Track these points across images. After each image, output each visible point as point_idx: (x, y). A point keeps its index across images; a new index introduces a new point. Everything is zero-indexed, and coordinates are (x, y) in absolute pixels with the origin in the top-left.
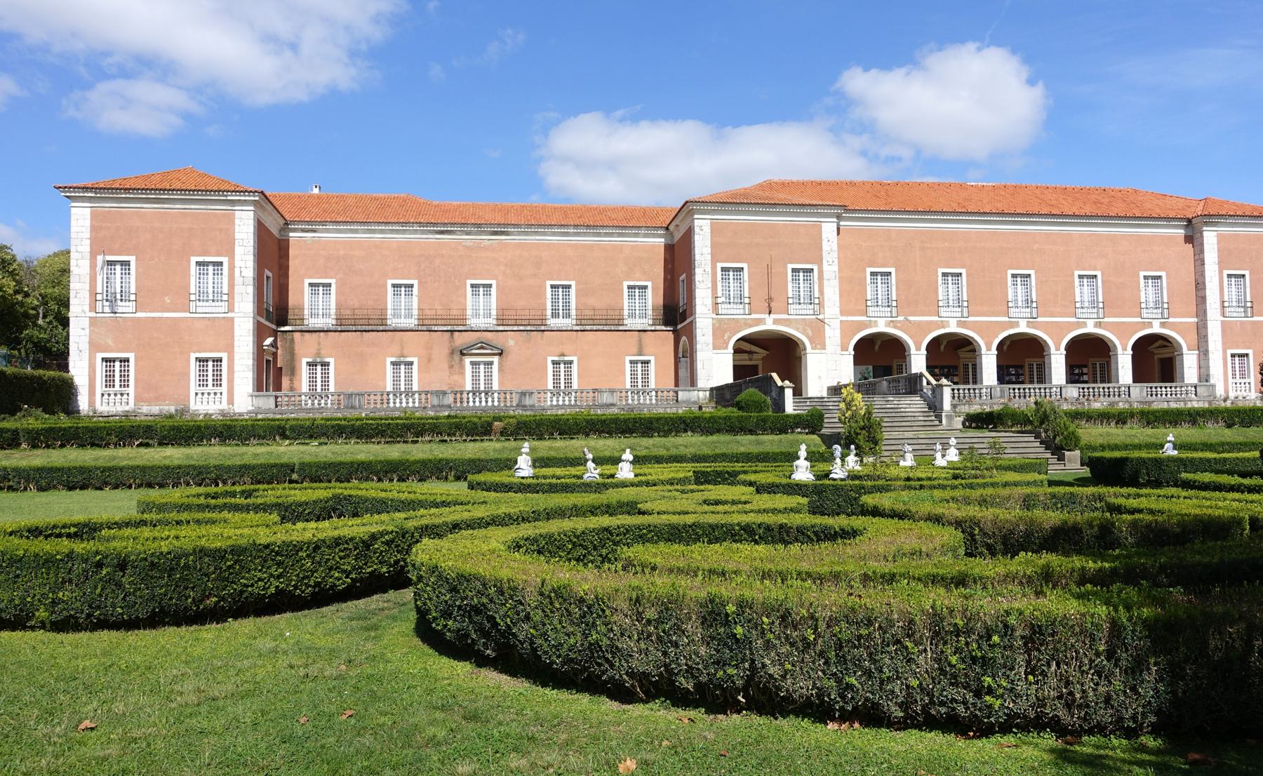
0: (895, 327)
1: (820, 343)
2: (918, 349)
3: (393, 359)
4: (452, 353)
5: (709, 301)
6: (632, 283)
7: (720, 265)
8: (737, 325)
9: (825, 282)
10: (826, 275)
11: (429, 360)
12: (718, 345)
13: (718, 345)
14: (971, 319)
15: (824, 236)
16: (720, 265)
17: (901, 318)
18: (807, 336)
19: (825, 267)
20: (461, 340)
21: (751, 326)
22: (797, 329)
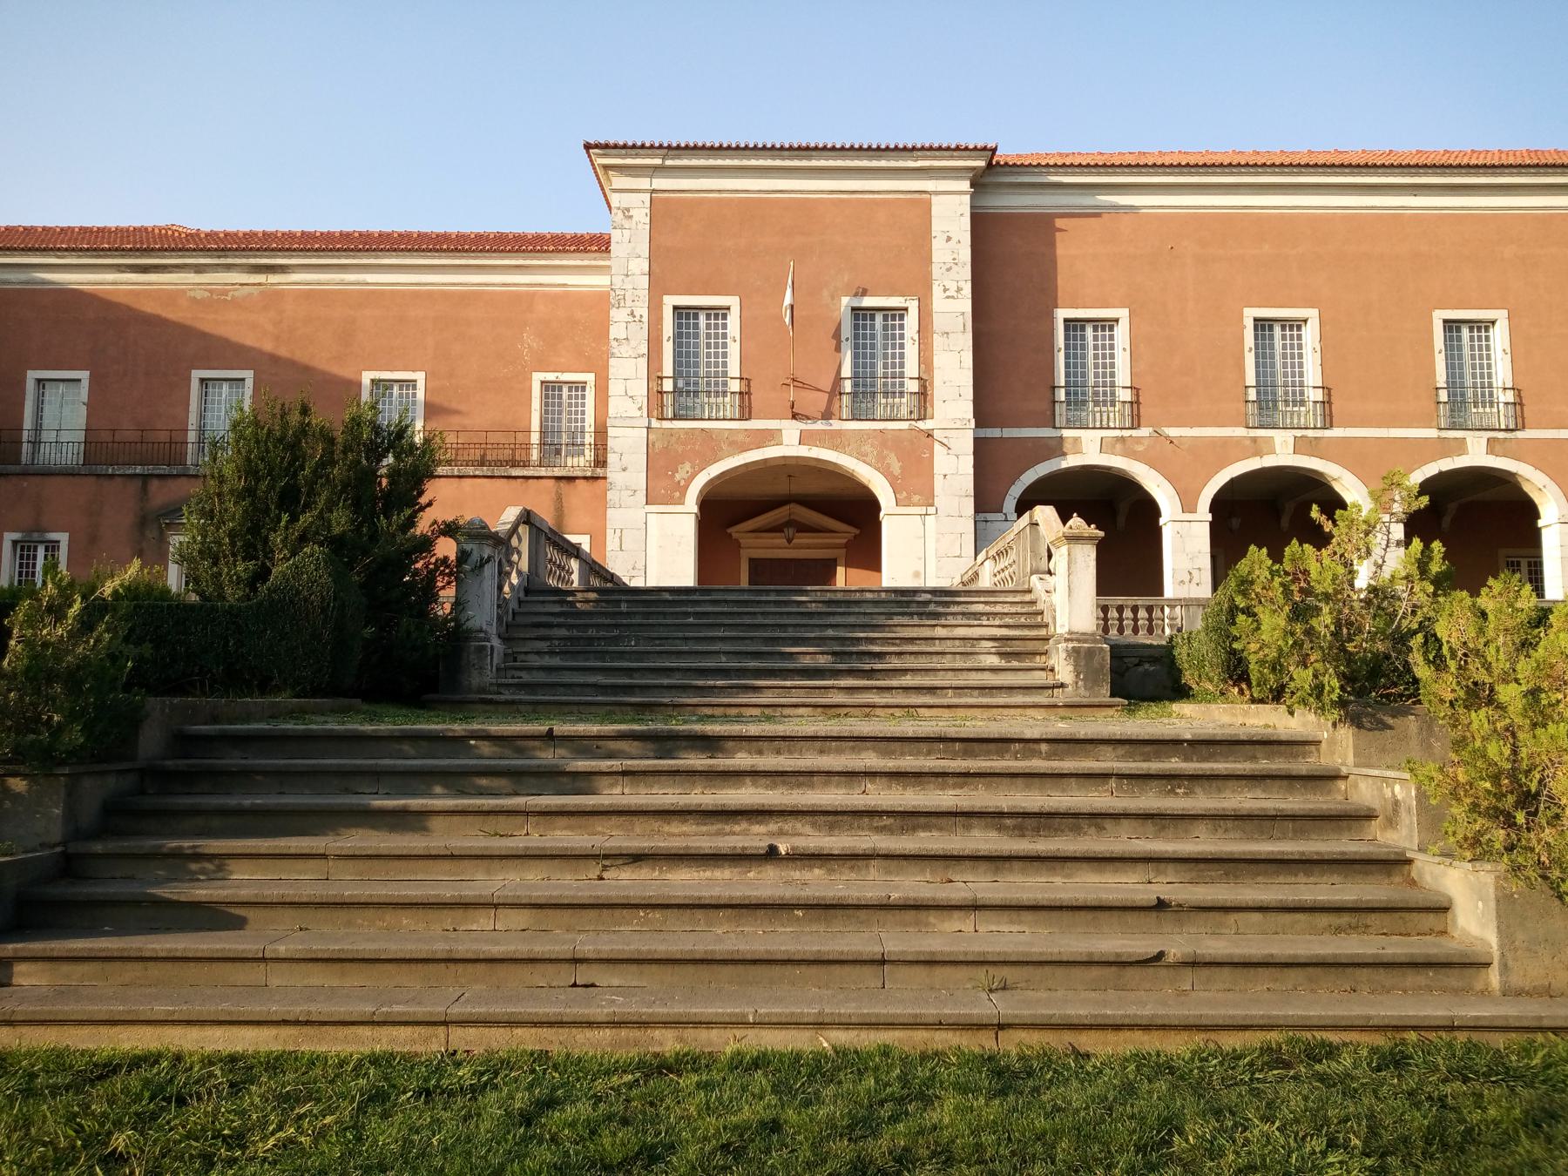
0: (1130, 454)
1: (918, 487)
2: (1188, 506)
3: (16, 536)
4: (143, 522)
5: (640, 388)
6: (551, 377)
7: (670, 301)
8: (711, 447)
9: (938, 340)
10: (938, 322)
11: (93, 539)
12: (660, 491)
13: (660, 491)
14: (1336, 432)
15: (937, 227)
16: (670, 301)
17: (1145, 432)
18: (887, 474)
19: (938, 302)
20: (161, 494)
21: (745, 448)
22: (862, 457)
